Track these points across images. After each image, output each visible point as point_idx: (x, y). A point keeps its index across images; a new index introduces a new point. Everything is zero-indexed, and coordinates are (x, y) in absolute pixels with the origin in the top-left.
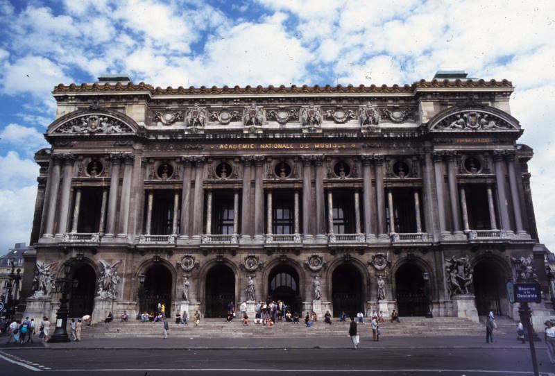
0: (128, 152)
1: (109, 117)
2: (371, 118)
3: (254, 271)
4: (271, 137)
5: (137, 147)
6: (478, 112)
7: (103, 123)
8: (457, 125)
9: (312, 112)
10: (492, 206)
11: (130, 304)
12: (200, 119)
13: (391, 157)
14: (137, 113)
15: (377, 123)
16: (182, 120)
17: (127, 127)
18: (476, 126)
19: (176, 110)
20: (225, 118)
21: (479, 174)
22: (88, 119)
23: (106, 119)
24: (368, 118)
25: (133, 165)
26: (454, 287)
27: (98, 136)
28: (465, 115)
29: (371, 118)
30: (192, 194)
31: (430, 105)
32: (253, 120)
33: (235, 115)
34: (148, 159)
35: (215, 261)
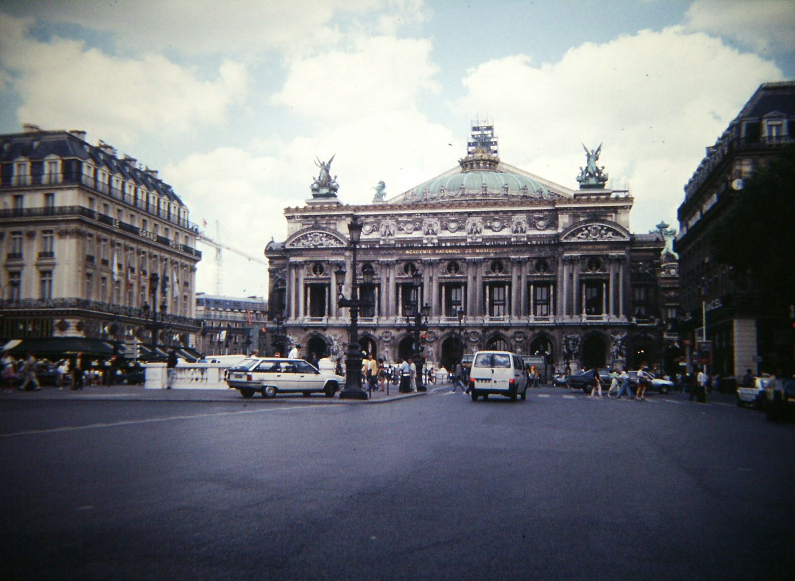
0: (340, 259)
3: (432, 342)
4: (443, 245)
7: (322, 238)
8: (581, 236)
9: (474, 225)
10: (604, 296)
13: (534, 258)
15: (525, 232)
16: (378, 230)
17: (339, 240)
18: (596, 237)
19: (372, 223)
20: (409, 228)
21: (598, 272)
22: (312, 235)
23: (325, 235)
27: (320, 248)
28: (589, 228)
30: (388, 287)
31: (566, 218)
32: (430, 231)
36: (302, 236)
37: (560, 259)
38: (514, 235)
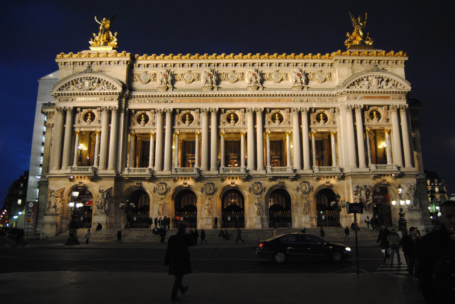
2: (299, 79)
22: (83, 80)
28: (370, 78)
34: (130, 110)
36: (72, 81)
38: (295, 85)
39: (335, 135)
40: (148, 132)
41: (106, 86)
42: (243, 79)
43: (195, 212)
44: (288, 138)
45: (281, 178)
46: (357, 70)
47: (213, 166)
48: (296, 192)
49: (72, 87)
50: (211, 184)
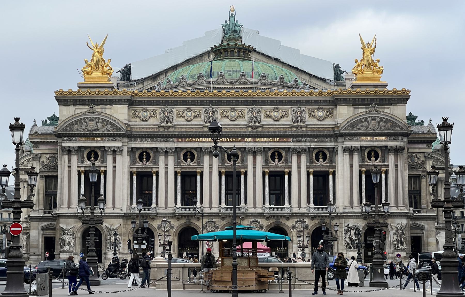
1: (102, 119)
2: (299, 118)
5: (126, 140)
6: (378, 117)
8: (361, 128)
11: (127, 254)
12: (170, 117)
14: (121, 113)
22: (87, 120)
24: (297, 118)
25: (122, 155)
26: (348, 244)
27: (96, 134)
28: (369, 119)
29: (299, 118)
33: (197, 113)
34: (132, 148)
35: (185, 224)
37: (340, 149)
38: (295, 124)
39: (334, 174)
40: (150, 170)
41: (109, 126)
42: (242, 116)
43: (197, 248)
44: (286, 177)
45: (277, 216)
46: (358, 108)
47: (213, 206)
48: (292, 230)
49: (76, 127)
50: (212, 221)
